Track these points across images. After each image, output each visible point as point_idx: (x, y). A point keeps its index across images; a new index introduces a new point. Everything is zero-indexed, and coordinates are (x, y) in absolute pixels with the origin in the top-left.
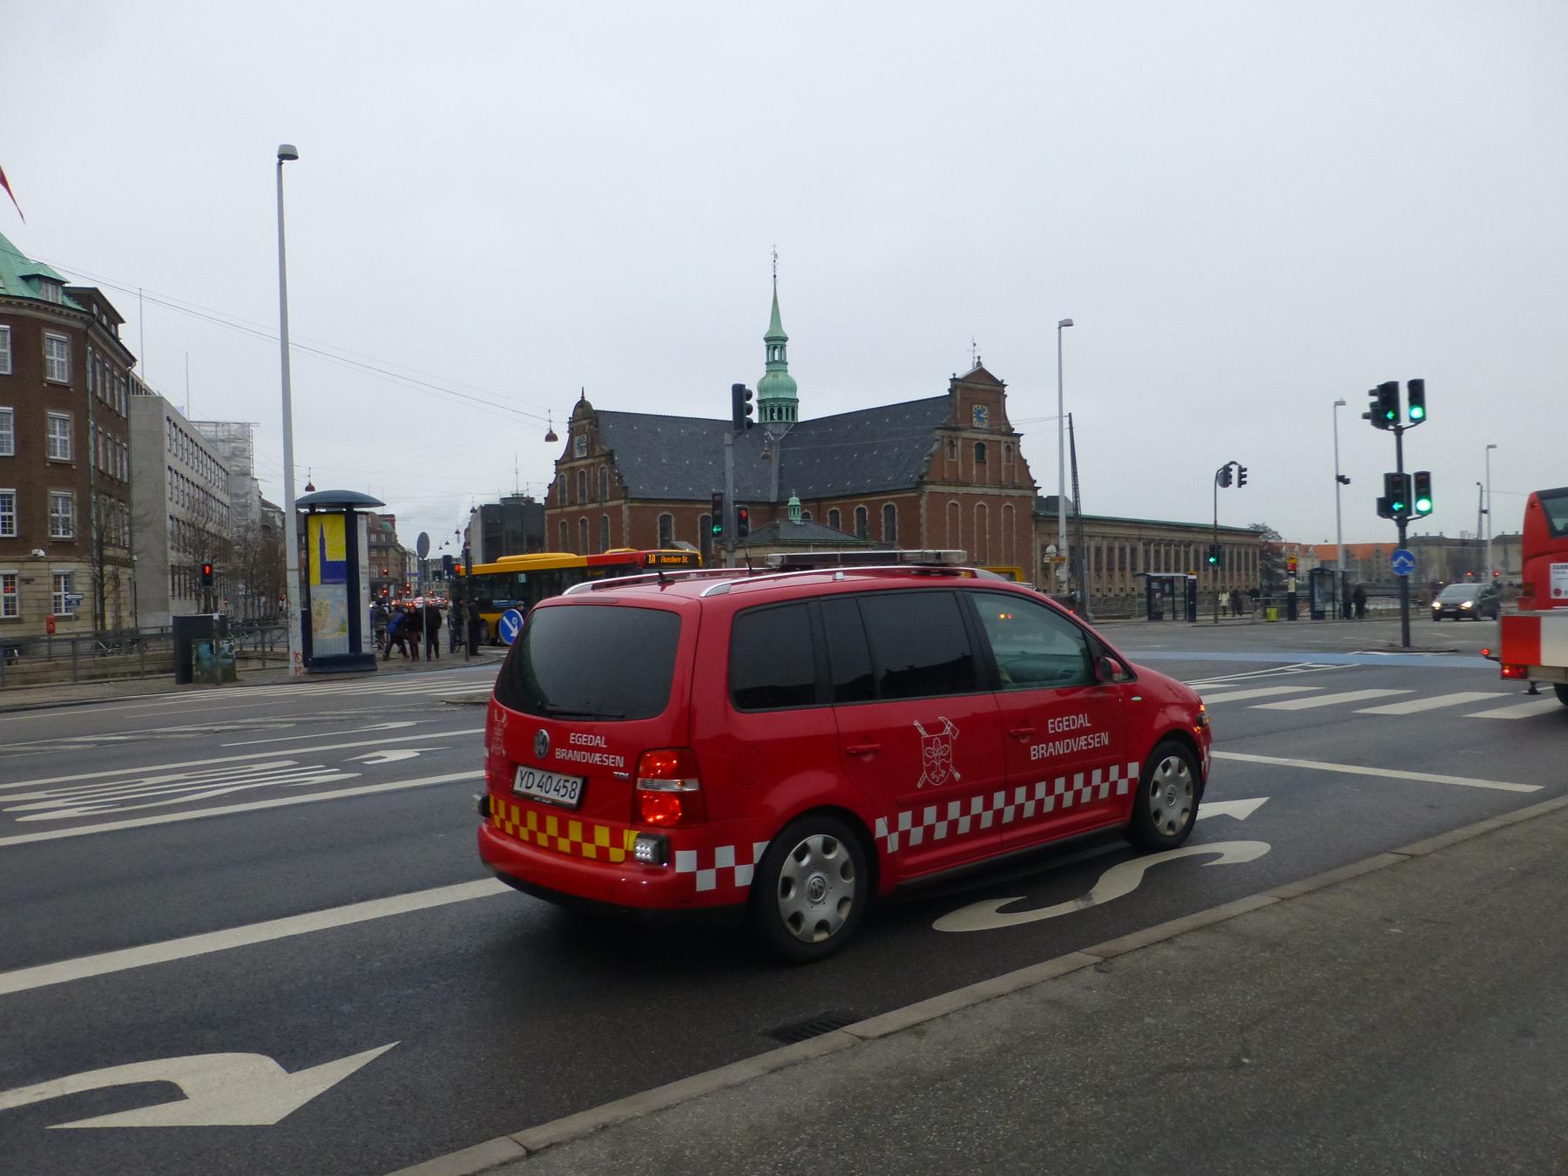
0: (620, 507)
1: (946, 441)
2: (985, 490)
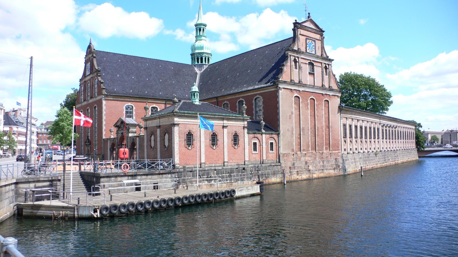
1: (293, 58)
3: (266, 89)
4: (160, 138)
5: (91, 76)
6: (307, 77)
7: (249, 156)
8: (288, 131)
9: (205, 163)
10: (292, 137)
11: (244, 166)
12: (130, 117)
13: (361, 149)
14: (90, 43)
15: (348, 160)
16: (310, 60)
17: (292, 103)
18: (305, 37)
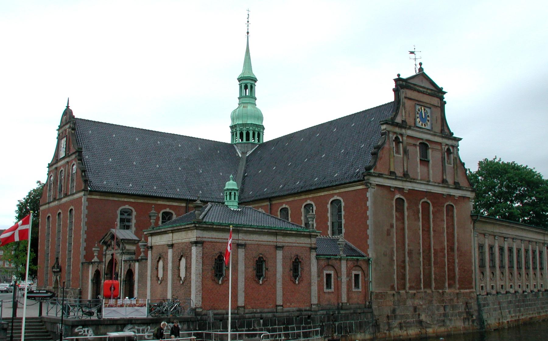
0: (80, 198)
1: (392, 137)
3: (349, 187)
4: (173, 265)
5: (66, 160)
6: (418, 167)
7: (319, 297)
8: (385, 255)
9: (244, 307)
10: (392, 265)
11: (310, 313)
12: (128, 227)
13: (511, 286)
14: (68, 107)
15: (488, 305)
16: (422, 139)
17: (392, 209)
18: (413, 103)
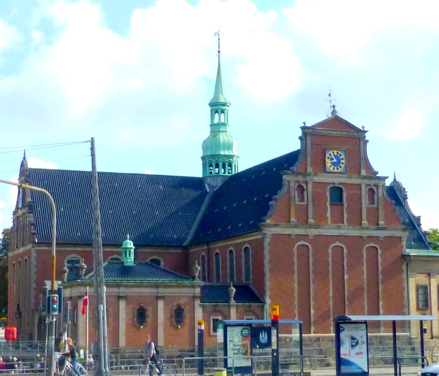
2: (342, 232)
